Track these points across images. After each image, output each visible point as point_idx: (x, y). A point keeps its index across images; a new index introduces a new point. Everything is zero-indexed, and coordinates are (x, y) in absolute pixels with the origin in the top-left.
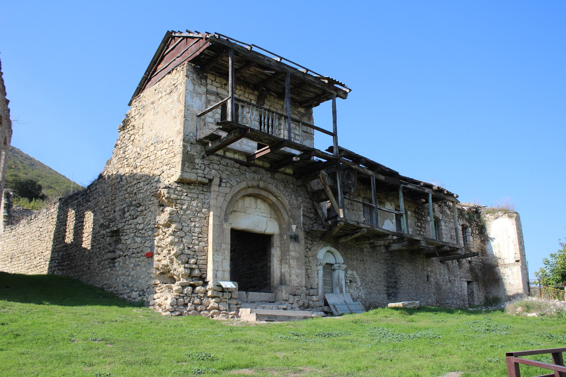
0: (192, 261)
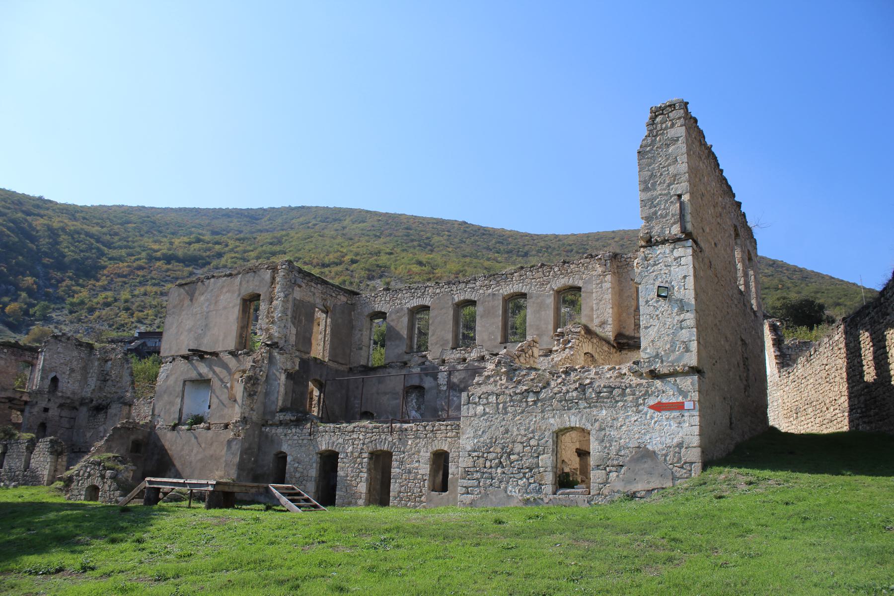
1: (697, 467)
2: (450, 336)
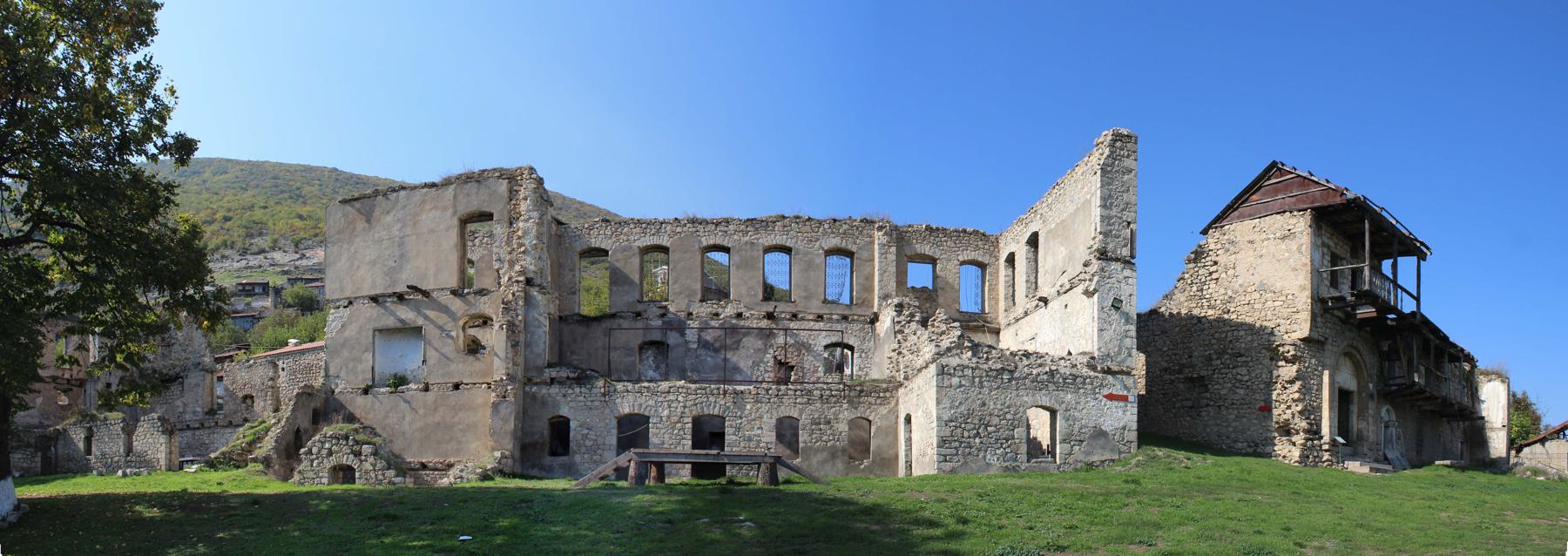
1: (1134, 445)
2: (698, 286)
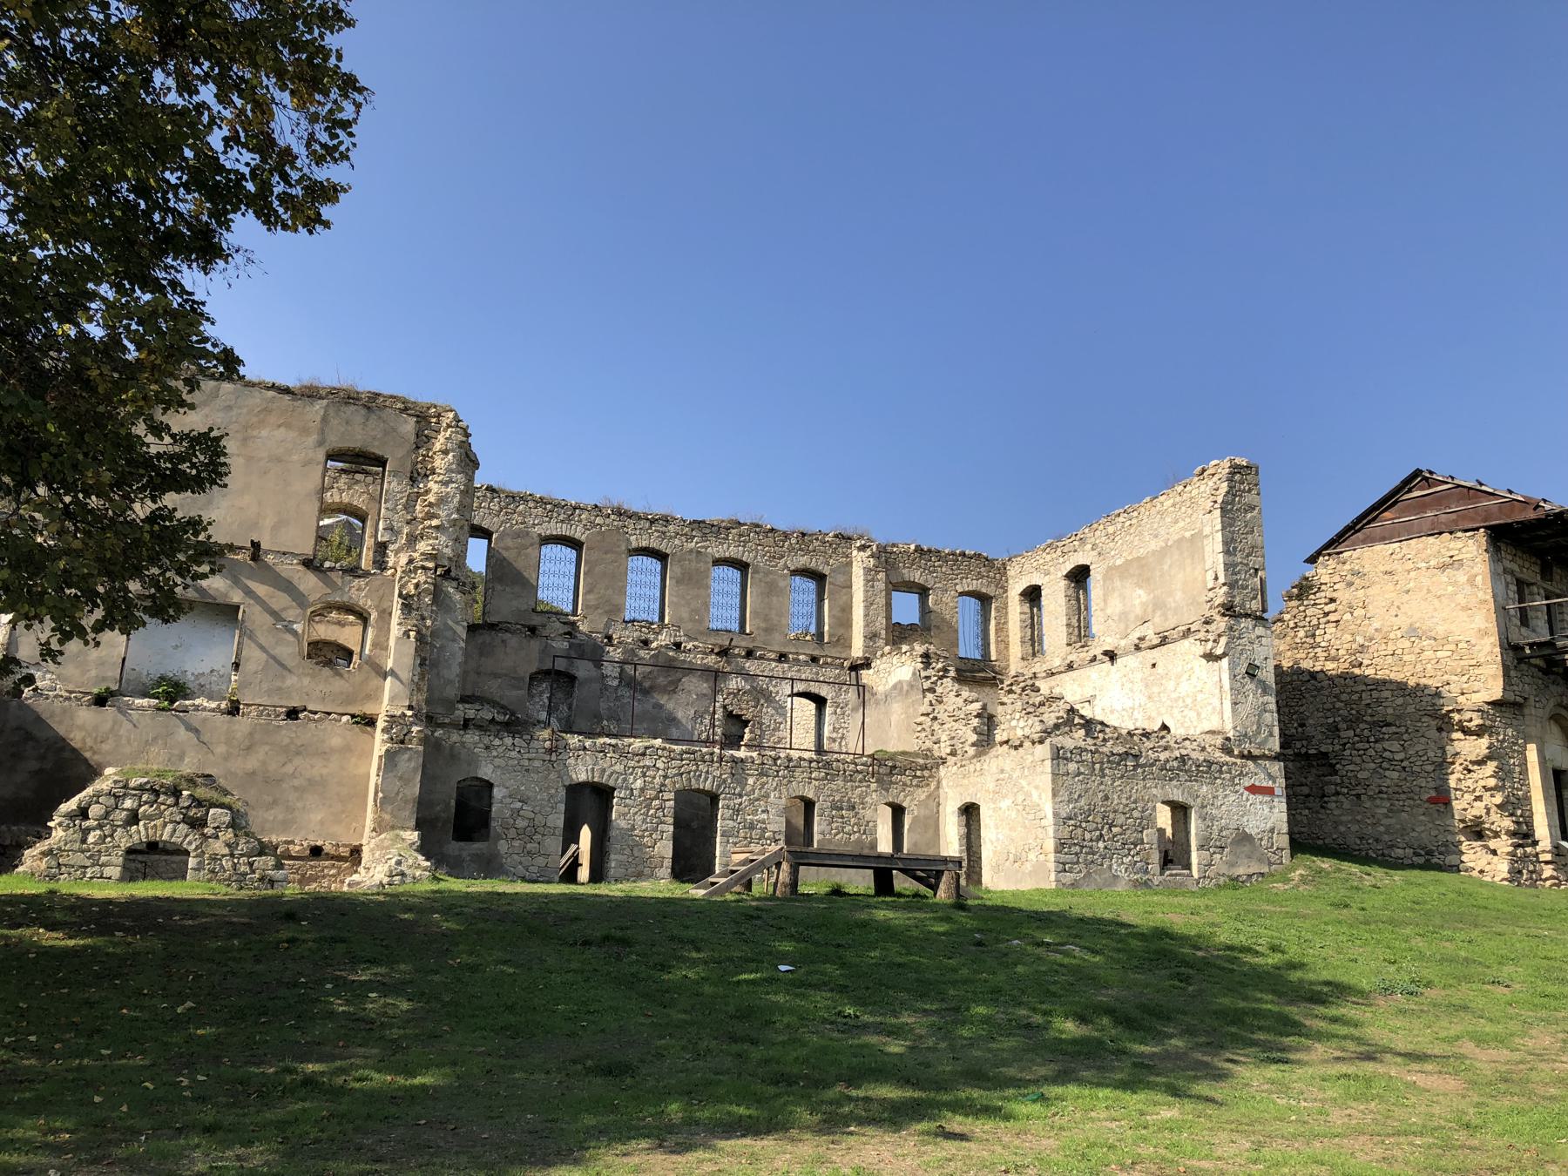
0: (1519, 812)
1: (1286, 853)
